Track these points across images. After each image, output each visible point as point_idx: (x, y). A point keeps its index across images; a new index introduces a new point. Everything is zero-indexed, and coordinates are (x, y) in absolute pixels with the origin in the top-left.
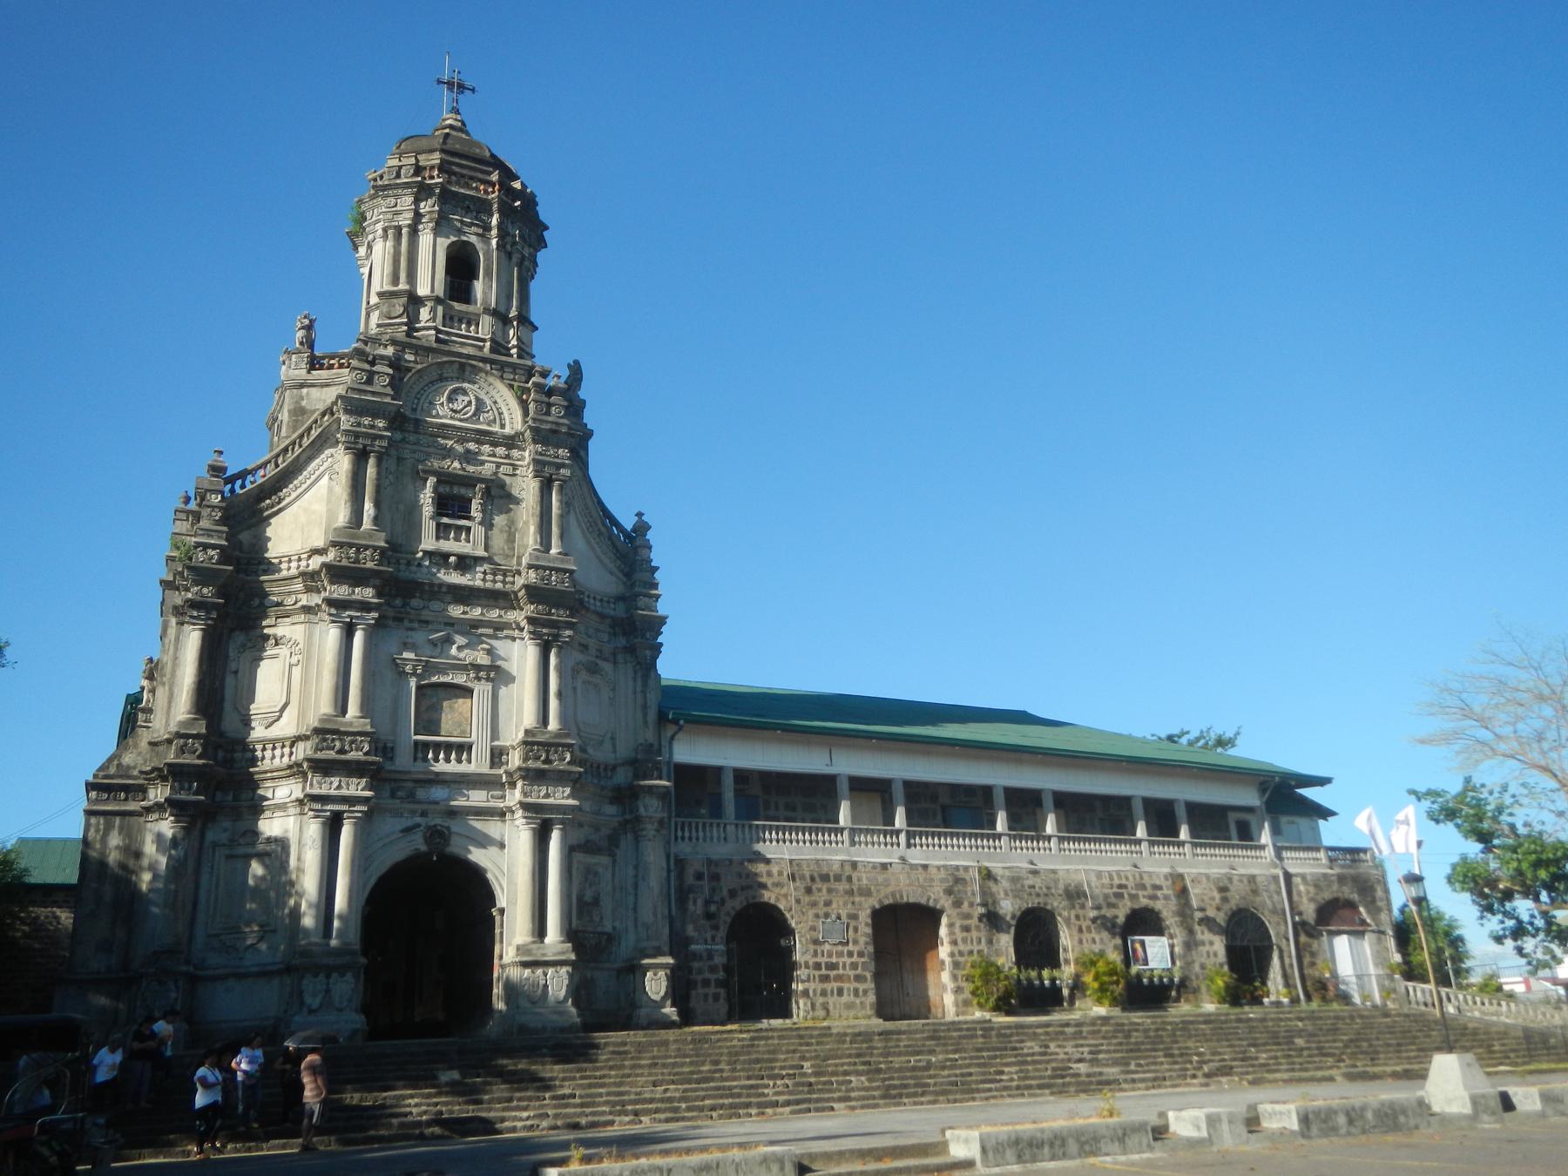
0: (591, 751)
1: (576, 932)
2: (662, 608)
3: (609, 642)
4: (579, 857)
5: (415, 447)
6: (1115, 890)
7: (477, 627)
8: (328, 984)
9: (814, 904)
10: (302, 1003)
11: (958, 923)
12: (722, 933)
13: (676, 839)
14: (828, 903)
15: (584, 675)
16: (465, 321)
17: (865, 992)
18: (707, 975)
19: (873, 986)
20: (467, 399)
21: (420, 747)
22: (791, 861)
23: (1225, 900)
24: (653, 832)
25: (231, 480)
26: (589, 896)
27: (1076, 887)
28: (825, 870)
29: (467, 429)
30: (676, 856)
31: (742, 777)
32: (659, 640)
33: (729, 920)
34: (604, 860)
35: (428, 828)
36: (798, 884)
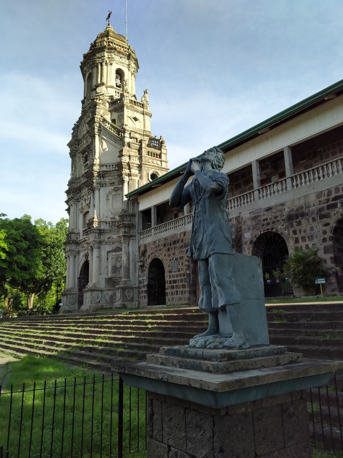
1: (110, 279)
6: (331, 202)
7: (89, 192)
9: (169, 255)
14: (174, 254)
15: (114, 193)
17: (185, 292)
19: (188, 289)
24: (123, 241)
27: (297, 210)
28: (175, 239)
33: (148, 267)
36: (166, 248)
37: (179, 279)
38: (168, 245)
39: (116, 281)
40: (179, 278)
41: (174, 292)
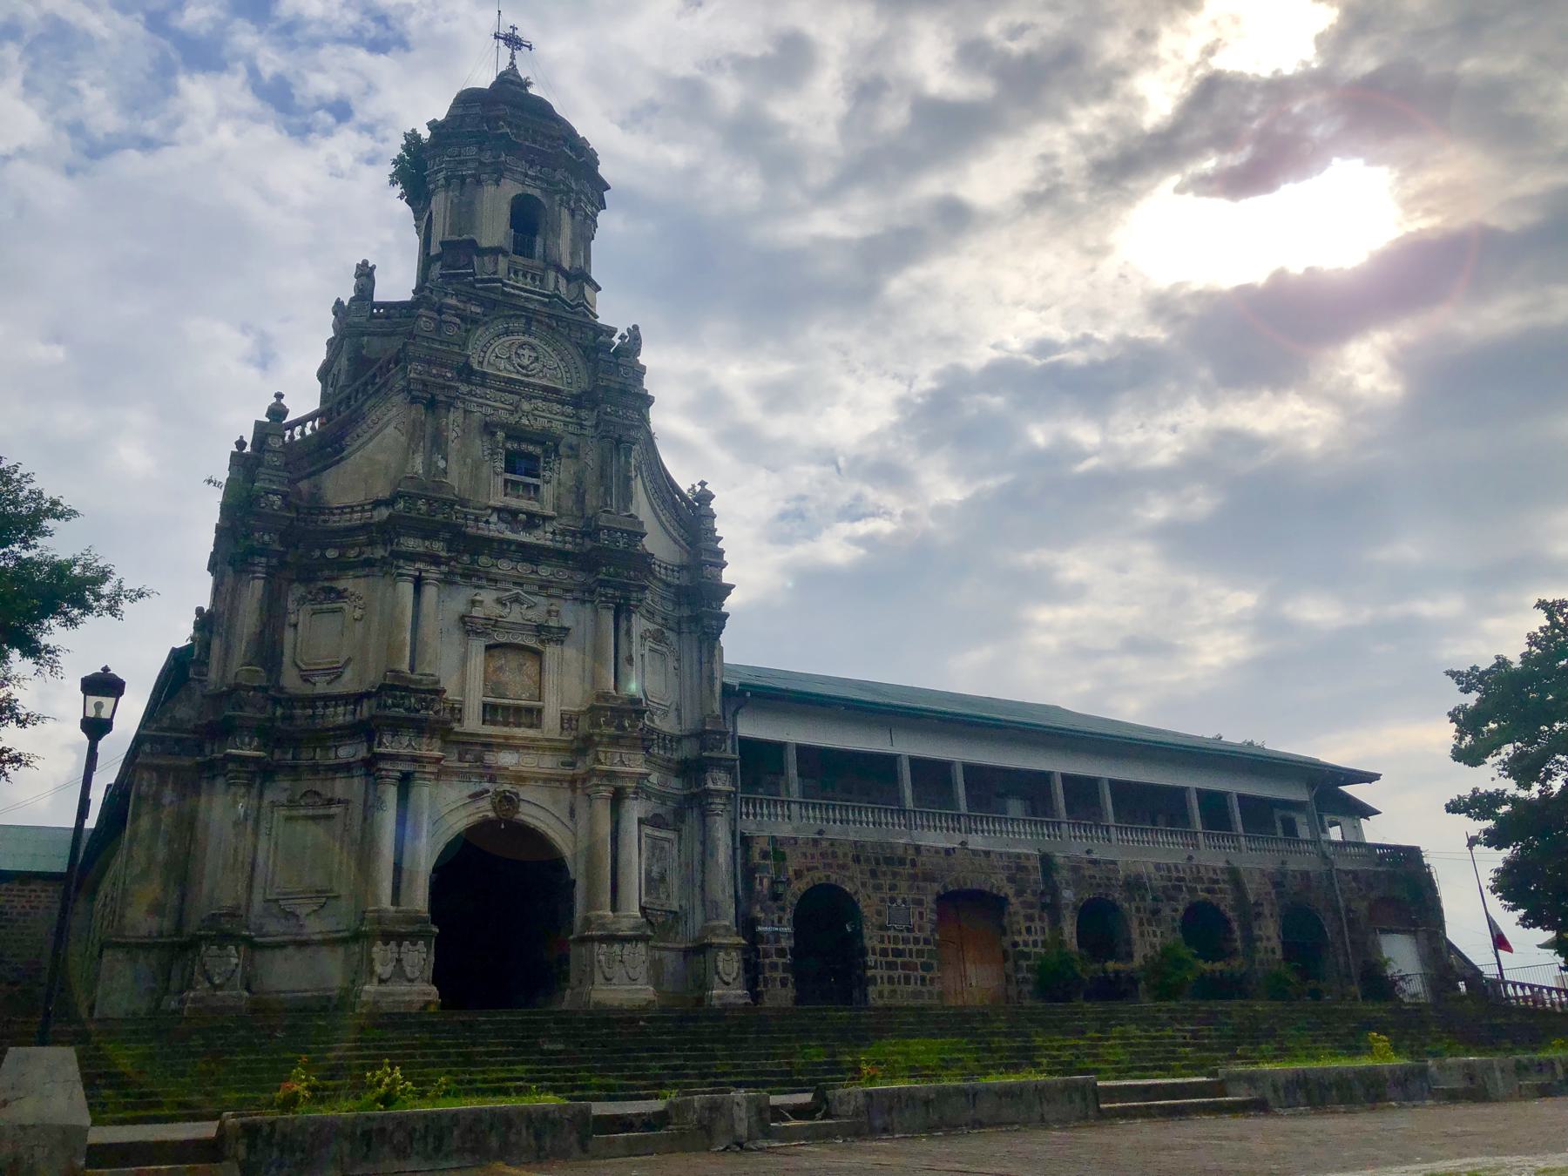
0: (657, 721)
2: (727, 576)
3: (673, 610)
4: (648, 830)
5: (480, 400)
7: (547, 588)
8: (399, 953)
9: (878, 888)
10: (372, 972)
11: (1022, 912)
12: (788, 916)
13: (741, 814)
14: (893, 888)
15: (649, 644)
16: (529, 276)
18: (775, 959)
20: (535, 355)
21: (488, 709)
22: (855, 842)
23: (1280, 895)
25: (291, 426)
26: (655, 870)
29: (534, 386)
30: (742, 833)
31: (806, 753)
32: (724, 609)
34: (671, 835)
35: (497, 793)
37: (910, 950)
38: (867, 860)
39: (653, 920)
40: (914, 948)
41: (896, 976)
